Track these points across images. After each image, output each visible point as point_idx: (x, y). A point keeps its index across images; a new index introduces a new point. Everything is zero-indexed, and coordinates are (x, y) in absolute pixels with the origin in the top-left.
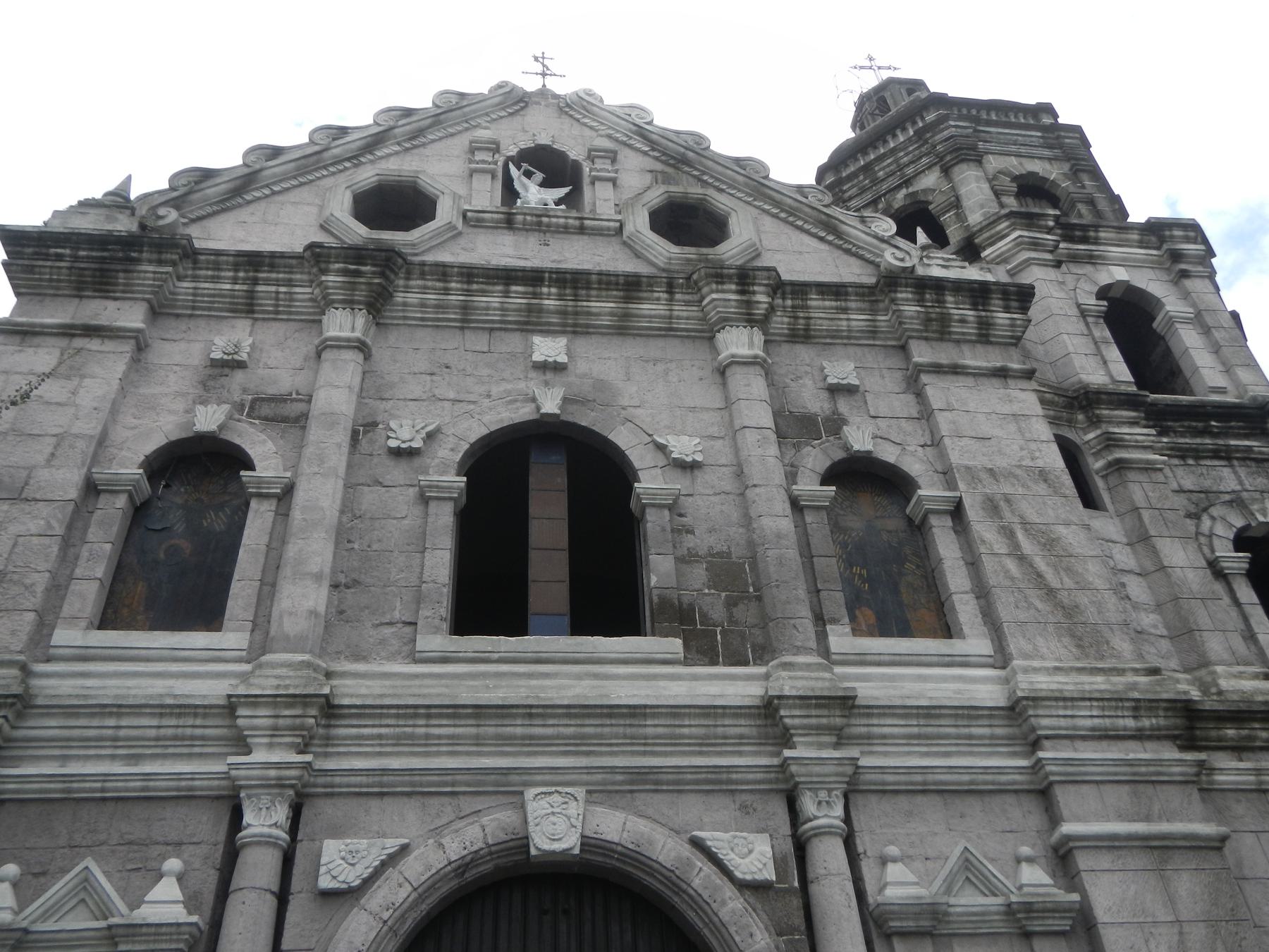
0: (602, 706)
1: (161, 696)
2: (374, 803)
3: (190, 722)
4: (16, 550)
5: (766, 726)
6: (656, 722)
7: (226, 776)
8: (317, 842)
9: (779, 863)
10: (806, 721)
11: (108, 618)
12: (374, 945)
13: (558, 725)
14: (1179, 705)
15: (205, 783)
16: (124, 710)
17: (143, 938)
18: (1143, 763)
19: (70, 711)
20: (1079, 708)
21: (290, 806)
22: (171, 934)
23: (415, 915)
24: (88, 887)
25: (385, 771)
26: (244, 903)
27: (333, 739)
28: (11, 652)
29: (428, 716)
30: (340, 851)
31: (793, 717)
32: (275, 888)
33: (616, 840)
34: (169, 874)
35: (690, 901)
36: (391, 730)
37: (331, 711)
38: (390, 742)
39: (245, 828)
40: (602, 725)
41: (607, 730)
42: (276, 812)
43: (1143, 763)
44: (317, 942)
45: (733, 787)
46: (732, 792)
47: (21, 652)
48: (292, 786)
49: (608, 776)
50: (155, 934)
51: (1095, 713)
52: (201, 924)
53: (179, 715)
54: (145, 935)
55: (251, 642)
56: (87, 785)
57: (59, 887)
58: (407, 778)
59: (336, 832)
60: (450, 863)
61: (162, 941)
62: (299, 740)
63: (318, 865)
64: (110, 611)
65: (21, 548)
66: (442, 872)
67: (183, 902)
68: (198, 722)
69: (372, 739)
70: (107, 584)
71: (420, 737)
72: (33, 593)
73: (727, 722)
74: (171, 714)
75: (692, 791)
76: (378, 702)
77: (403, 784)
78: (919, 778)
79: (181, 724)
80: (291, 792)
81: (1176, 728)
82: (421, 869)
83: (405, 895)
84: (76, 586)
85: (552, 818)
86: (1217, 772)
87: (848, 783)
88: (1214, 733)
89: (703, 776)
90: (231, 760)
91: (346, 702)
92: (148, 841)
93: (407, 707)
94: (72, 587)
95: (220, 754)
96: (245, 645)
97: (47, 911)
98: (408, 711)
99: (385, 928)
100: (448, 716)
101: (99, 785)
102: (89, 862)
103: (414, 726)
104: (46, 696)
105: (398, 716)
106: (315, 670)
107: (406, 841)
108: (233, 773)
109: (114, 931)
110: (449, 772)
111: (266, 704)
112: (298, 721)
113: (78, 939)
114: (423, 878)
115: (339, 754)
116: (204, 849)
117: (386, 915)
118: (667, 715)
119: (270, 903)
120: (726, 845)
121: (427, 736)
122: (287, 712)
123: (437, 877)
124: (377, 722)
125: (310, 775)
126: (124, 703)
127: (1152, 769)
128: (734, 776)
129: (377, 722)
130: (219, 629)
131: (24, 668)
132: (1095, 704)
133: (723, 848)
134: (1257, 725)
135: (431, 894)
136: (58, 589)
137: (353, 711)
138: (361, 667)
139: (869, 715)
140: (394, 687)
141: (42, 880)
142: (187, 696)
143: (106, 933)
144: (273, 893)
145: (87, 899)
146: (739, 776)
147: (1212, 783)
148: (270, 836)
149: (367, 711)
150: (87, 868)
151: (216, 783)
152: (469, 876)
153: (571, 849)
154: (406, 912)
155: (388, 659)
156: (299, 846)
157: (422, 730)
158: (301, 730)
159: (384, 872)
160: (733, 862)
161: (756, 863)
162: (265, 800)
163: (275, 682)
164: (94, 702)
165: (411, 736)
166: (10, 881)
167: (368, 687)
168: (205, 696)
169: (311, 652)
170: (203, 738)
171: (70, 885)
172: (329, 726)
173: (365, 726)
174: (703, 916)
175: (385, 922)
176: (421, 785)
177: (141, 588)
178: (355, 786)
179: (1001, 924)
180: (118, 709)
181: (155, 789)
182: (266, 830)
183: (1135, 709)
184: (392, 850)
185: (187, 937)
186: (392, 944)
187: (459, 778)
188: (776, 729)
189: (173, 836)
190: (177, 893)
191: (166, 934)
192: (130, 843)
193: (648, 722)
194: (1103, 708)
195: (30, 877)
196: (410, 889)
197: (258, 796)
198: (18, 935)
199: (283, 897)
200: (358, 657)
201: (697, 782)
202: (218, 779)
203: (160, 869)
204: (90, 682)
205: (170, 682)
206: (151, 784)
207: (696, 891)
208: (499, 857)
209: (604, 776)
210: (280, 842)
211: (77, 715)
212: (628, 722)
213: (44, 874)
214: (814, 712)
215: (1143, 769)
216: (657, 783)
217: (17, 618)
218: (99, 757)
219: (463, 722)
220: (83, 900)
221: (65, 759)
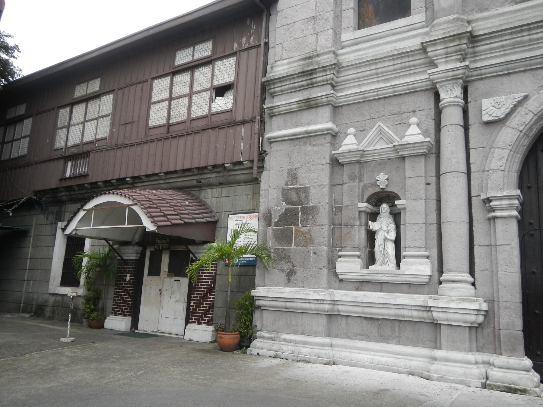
1: (391, 51)
2: (505, 79)
3: (407, 59)
4: (317, 6)
7: (429, 80)
8: (479, 102)
11: (361, 24)
15: (419, 84)
16: (377, 61)
17: (408, 149)
19: (357, 66)
21: (462, 88)
22: (420, 146)
23: (537, 127)
24: (382, 133)
25: (508, 62)
26: (449, 131)
27: (477, 53)
28: (328, 48)
29: (529, 30)
30: (491, 103)
32: (462, 124)
34: (413, 124)
36: (509, 41)
37: (474, 39)
38: (509, 48)
39: (442, 100)
42: (455, 91)
44: (487, 144)
47: (331, 47)
48: (461, 78)
50: (413, 147)
52: (431, 142)
53: (401, 58)
54: (409, 148)
55: (426, 17)
56: (371, 94)
57: (371, 134)
58: (522, 63)
59: (487, 95)
61: (416, 149)
62: (460, 56)
63: (481, 111)
64: (361, 22)
65: (319, 4)
67: (422, 134)
68: (410, 59)
69: (499, 49)
70: (357, 10)
71: (526, 42)
72: (329, 22)
74: (398, 58)
76: (499, 29)
79: (403, 61)
80: (461, 81)
82: (538, 105)
83: (530, 118)
84: (344, 14)
90: (429, 72)
91: (481, 33)
92: (401, 113)
93: (516, 27)
94: (343, 15)
95: (423, 71)
96: (424, 19)
97: (369, 143)
98: (517, 29)
99: (522, 134)
101: (375, 93)
102: (379, 123)
103: (521, 37)
104: (346, 62)
105: (511, 33)
106: (461, 21)
107: (526, 93)
108: (432, 77)
109: (396, 147)
111: (440, 43)
112: (458, 48)
113: (384, 152)
114: (540, 109)
115: (481, 59)
116: (426, 112)
119: (461, 131)
121: (530, 40)
122: (451, 45)
124: (500, 39)
125: (469, 72)
126: (377, 58)
130: (410, 15)
131: (334, 53)
136: (338, 17)
137: (486, 36)
138: (486, 14)
140: (506, 19)
141: (364, 132)
142: (403, 48)
143: (393, 149)
144: (461, 126)
145: (383, 138)
148: (455, 102)
149: (493, 35)
150: (379, 125)
151: (424, 83)
154: (532, 126)
155: (500, 6)
156: (469, 104)
157: (527, 38)
158: (460, 51)
159: (516, 110)
162: (449, 86)
163: (443, 31)
164: (365, 60)
165: (521, 42)
166: (353, 134)
167: (491, 23)
168: (411, 47)
169: (457, 13)
170: (414, 66)
171: (375, 133)
173: (493, 43)
175: (521, 131)
176: (531, 65)
177: (371, 7)
178: (493, 73)
180: (375, 61)
181: (398, 91)
182: (452, 99)
184: (519, 99)
185: (427, 147)
186: (527, 141)
189: (411, 109)
190: (418, 131)
191: (418, 147)
192: (394, 114)
195: (359, 132)
196: (533, 115)
197: (445, 85)
198: (361, 152)
199: (466, 127)
200: (483, 10)
202: (425, 81)
203: (409, 123)
204: (361, 53)
205: (394, 45)
206: (397, 89)
211: (359, 67)
213: (364, 130)
217: (326, 33)
218: (373, 82)
220: (381, 138)
221: (359, 86)
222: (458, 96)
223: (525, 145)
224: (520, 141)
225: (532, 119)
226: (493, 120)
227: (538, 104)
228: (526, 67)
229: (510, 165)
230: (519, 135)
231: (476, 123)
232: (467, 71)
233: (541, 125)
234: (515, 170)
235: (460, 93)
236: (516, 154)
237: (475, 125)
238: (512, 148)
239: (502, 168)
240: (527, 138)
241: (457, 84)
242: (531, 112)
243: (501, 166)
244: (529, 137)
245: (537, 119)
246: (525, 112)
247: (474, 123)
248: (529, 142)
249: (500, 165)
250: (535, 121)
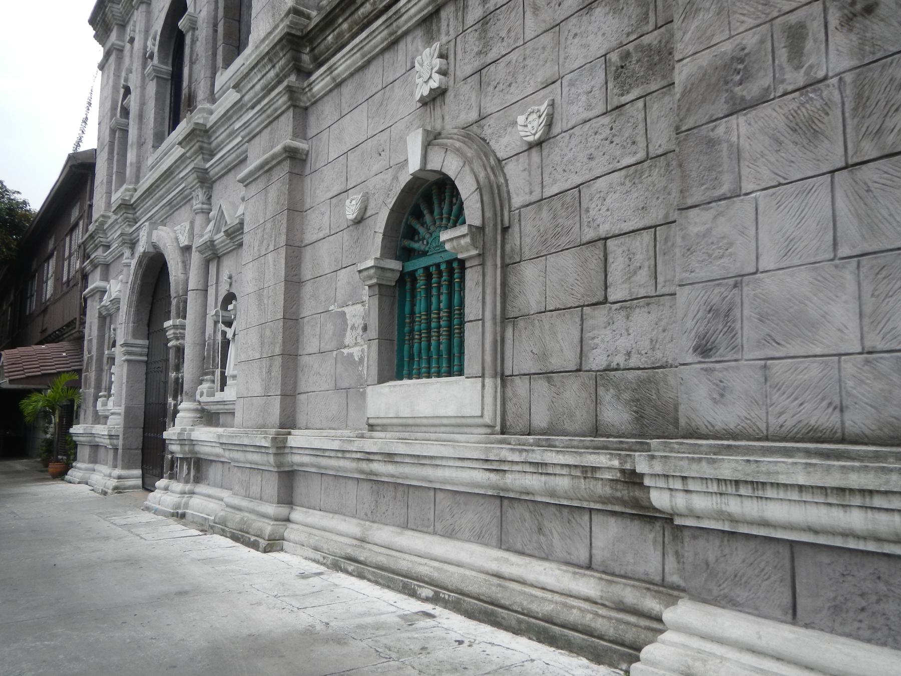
14: (284, 41)
18: (267, 107)
20: (251, 79)
43: (267, 107)
51: (259, 77)
78: (223, 165)
81: (288, 62)
86: (313, 84)
87: (199, 182)
88: (322, 46)
100: (148, 196)
127: (272, 108)
132: (255, 70)
134: (340, 20)
139: (214, 132)
147: (313, 96)
179: (231, 244)
183: (270, 60)
194: (259, 71)
215: (269, 112)
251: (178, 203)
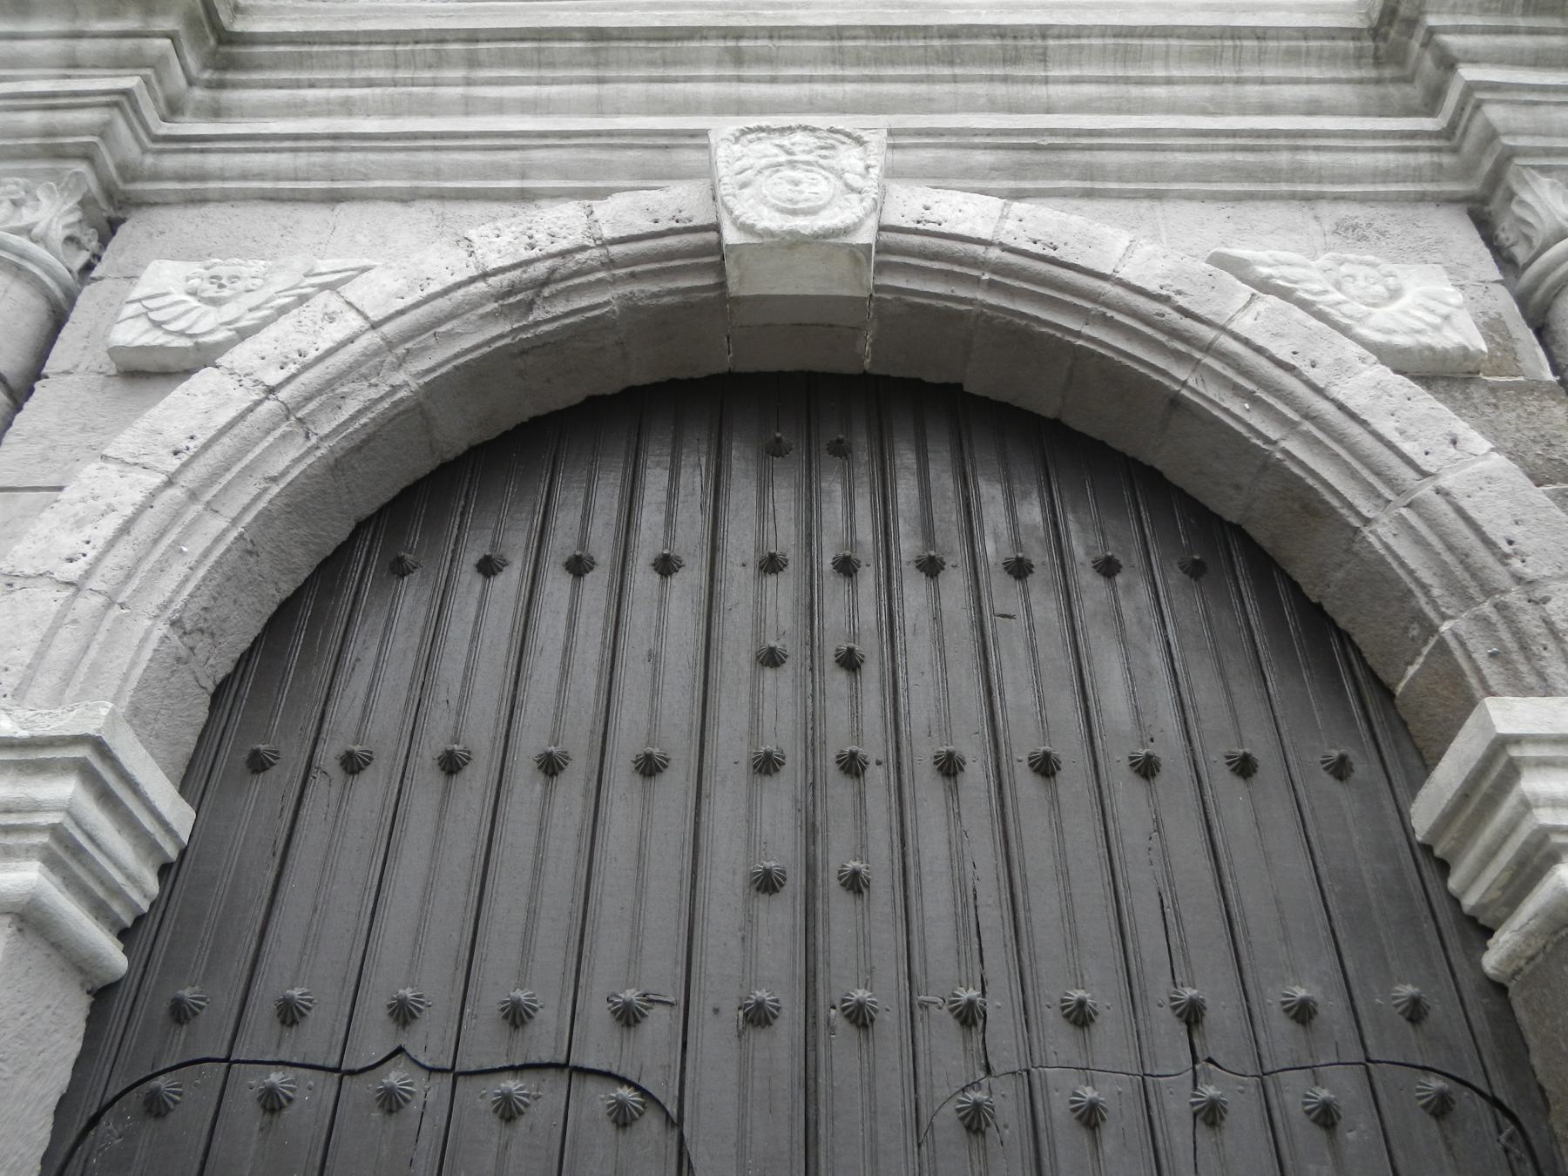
0: (925, 31)
2: (312, 218)
5: (1378, 81)
6: (1075, 72)
9: (1492, 327)
10: (1501, 41)
12: (226, 440)
13: (811, 79)
29: (472, 62)
30: (188, 279)
31: (1463, 30)
33: (985, 232)
35: (1229, 373)
36: (378, 91)
37: (224, 49)
40: (929, 79)
41: (939, 89)
45: (1312, 188)
46: (1308, 198)
49: (953, 154)
60: (485, 276)
66: (459, 295)
73: (1270, 72)
75: (1189, 197)
77: (390, 173)
85: (787, 173)
89: (1224, 157)
93: (415, 37)
100: (522, 61)
110: (512, 142)
112: (127, 44)
117: (273, 377)
118: (1104, 55)
120: (1317, 275)
123: (443, 304)
124: (342, 75)
125: (145, 151)
128: (1312, 158)
129: (342, 75)
133: (1310, 280)
135: (425, 349)
146: (1325, 158)
152: (551, 313)
153: (846, 231)
154: (341, 376)
160: (1345, 308)
161: (1419, 314)
172: (221, 85)
173: (312, 85)
174: (1280, 406)
175: (271, 390)
178: (261, 176)
186: (294, 453)
187: (538, 155)
188: (1407, 89)
193: (1055, 72)
201: (1204, 173)
207: (1246, 342)
208: (633, 275)
209: (941, 153)
210: (37, 271)
212: (998, 71)
214: (1522, 22)
216: (1089, 173)
219: (560, 73)
222: (36, 231)
223: (274, 473)
224: (248, 444)
225: (351, 340)
226: (162, 348)
227: (402, 281)
228: (416, 179)
229: (139, 560)
230: (250, 410)
231: (82, 368)
232: (121, 126)
233: (395, 389)
234: (164, 607)
235: (58, 233)
236: (199, 507)
237: (69, 378)
238: (185, 465)
239: (74, 571)
240: (300, 440)
241: (58, 185)
242: (358, 310)
243: (71, 560)
244: (314, 440)
245: (377, 353)
246: (326, 306)
247: (67, 366)
248: (301, 467)
249: (67, 553)
250: (368, 355)
251: (1150, 173)
